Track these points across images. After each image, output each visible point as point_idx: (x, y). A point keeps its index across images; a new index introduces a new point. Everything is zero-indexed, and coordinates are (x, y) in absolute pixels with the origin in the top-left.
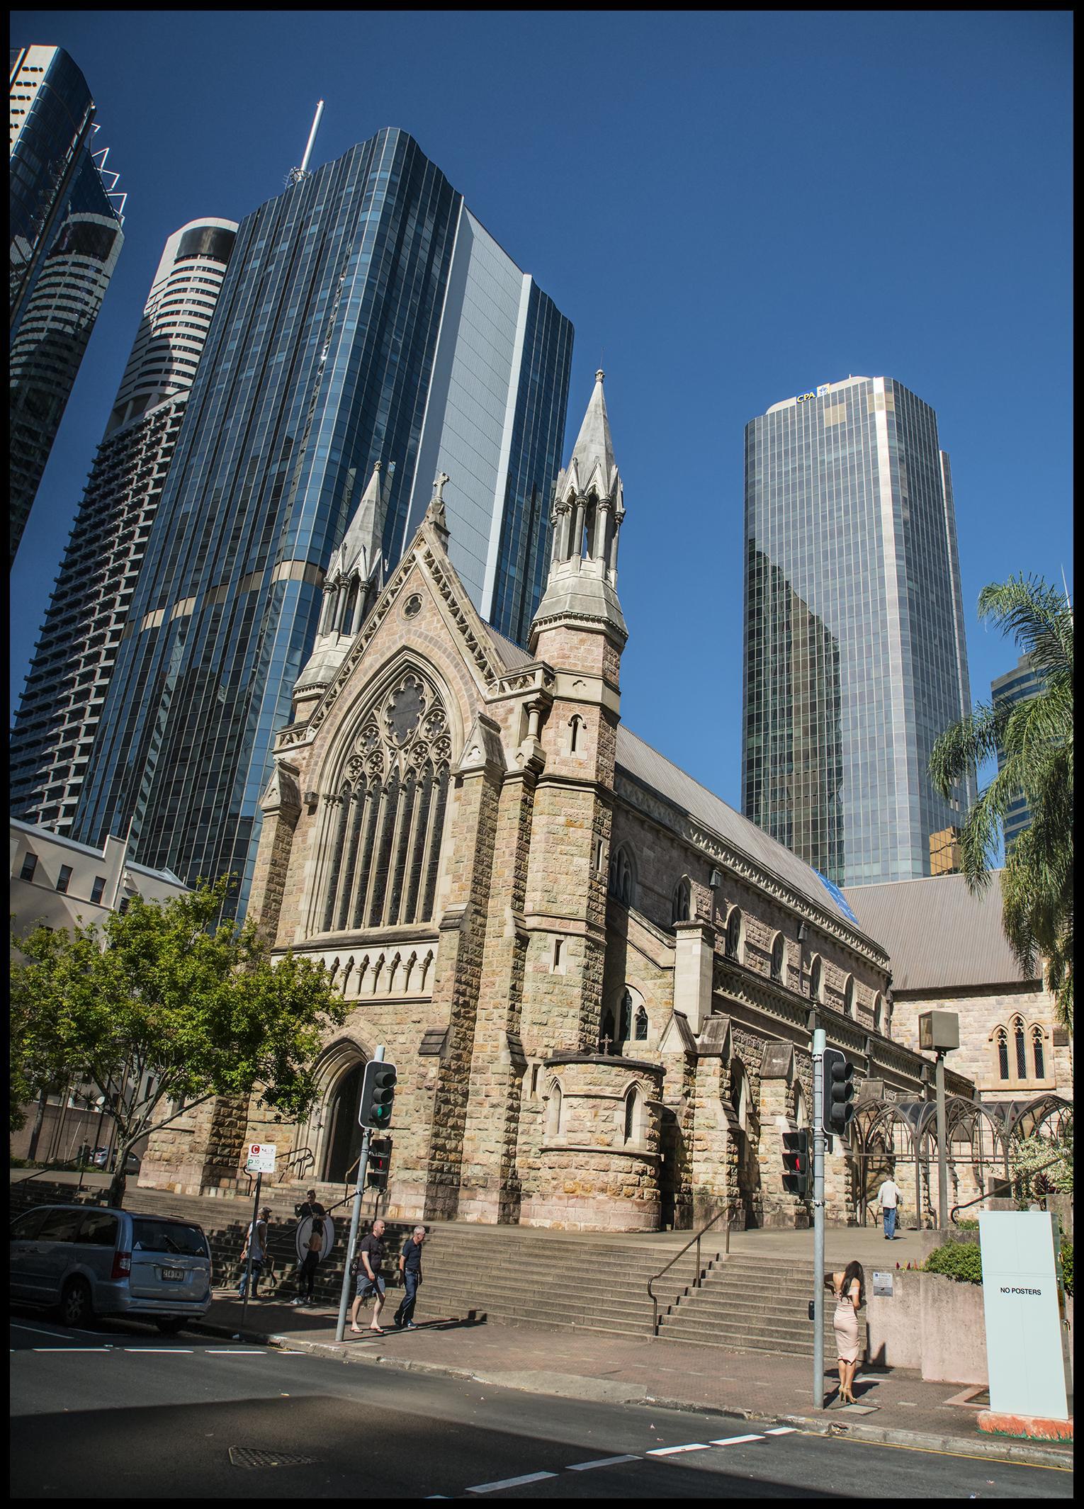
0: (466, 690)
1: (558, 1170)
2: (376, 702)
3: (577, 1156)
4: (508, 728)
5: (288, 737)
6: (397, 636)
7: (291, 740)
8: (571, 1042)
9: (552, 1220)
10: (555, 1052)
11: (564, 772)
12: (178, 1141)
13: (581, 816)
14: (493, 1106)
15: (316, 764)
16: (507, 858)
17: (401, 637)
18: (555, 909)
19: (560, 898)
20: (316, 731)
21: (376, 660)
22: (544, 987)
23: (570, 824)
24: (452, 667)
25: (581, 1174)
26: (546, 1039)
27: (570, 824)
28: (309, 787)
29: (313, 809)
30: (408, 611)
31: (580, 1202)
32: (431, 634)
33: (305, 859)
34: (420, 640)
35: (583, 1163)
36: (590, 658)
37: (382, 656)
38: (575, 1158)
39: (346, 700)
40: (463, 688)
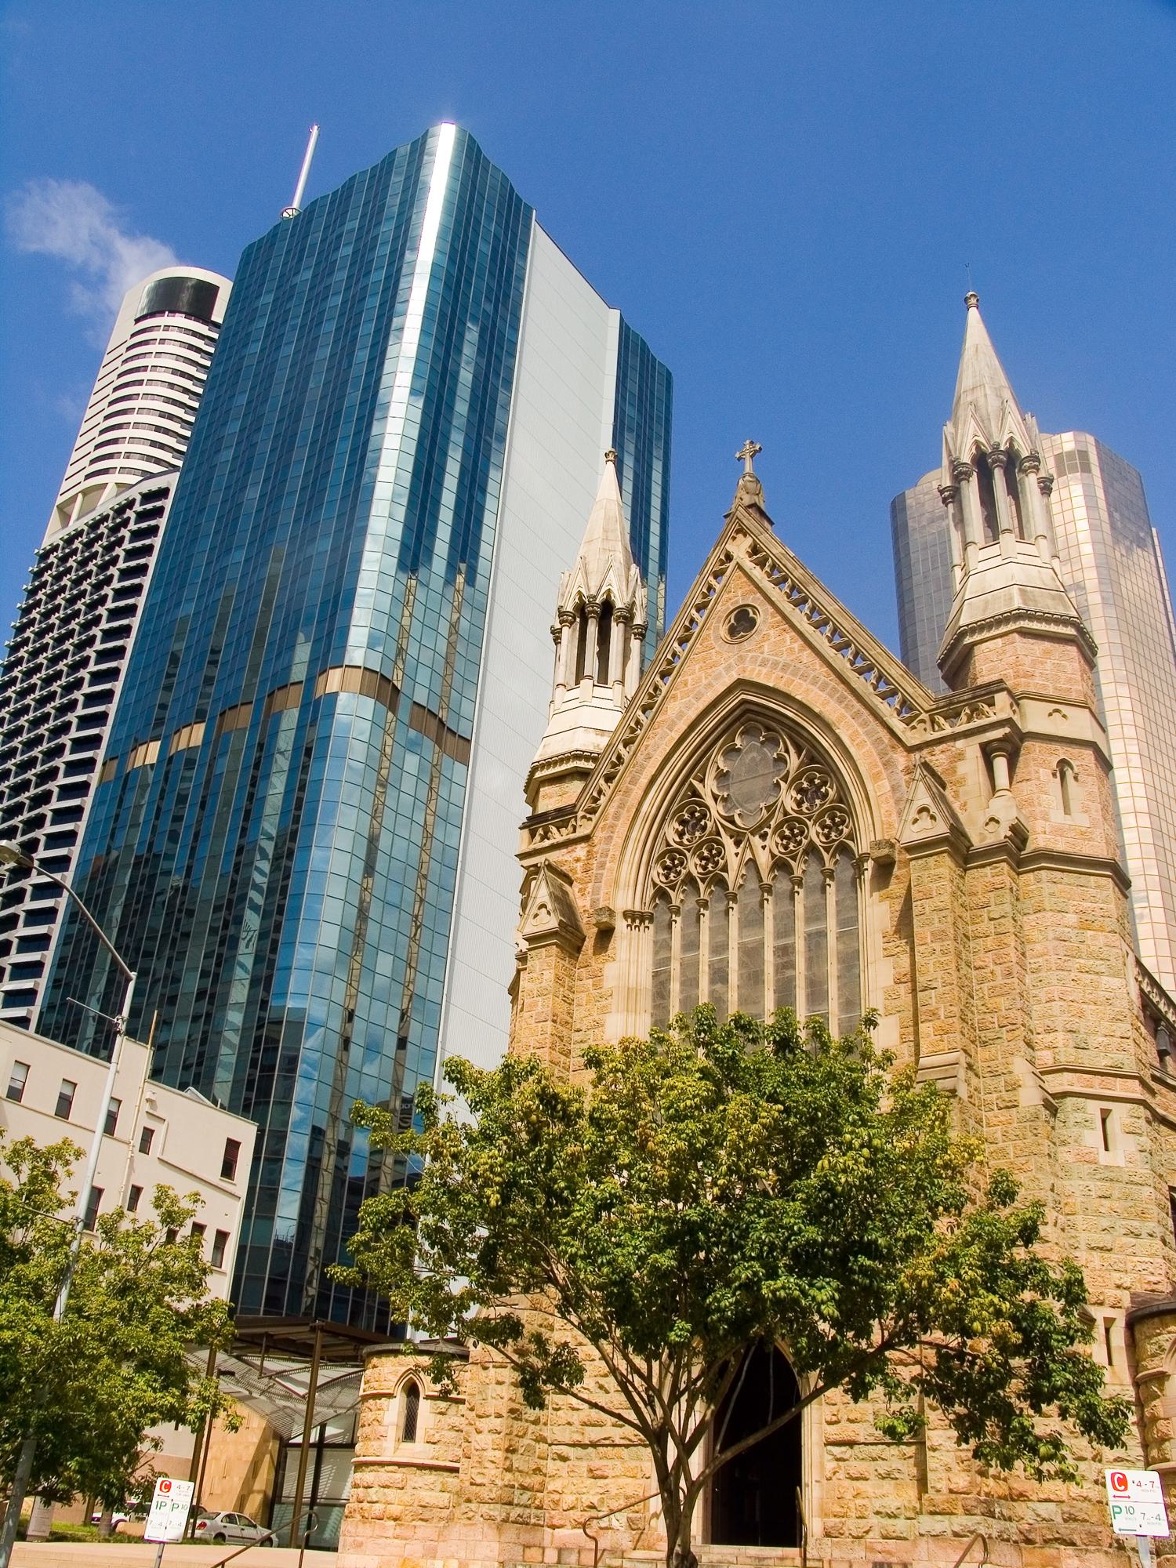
0: (867, 733)
2: (697, 766)
4: (961, 782)
5: (541, 831)
6: (721, 668)
7: (545, 837)
8: (1154, 1279)
10: (1134, 1296)
11: (1060, 846)
12: (411, 1484)
13: (1098, 913)
15: (602, 866)
16: (1000, 980)
17: (728, 668)
18: (1087, 1060)
19: (1094, 1041)
20: (595, 817)
22: (1098, 1188)
23: (1085, 925)
24: (833, 703)
26: (1117, 1275)
27: (1085, 925)
28: (594, 902)
30: (732, 631)
32: (783, 659)
33: (604, 1011)
34: (764, 670)
36: (1063, 676)
37: (697, 698)
39: (643, 767)
40: (860, 730)
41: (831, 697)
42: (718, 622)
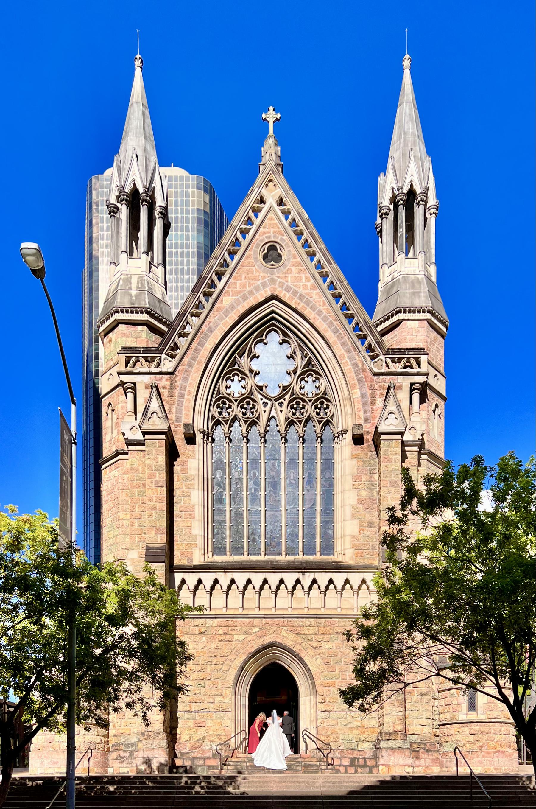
0: (350, 358)
1: (480, 735)
3: (494, 726)
5: (133, 360)
6: (259, 283)
9: (483, 767)
14: (422, 694)
17: (264, 285)
21: (238, 302)
25: (497, 737)
29: (191, 440)
30: (265, 257)
31: (502, 755)
32: (301, 291)
35: (498, 730)
37: (245, 298)
38: (492, 728)
39: (207, 337)
40: (346, 355)
41: (330, 327)
42: (257, 247)
